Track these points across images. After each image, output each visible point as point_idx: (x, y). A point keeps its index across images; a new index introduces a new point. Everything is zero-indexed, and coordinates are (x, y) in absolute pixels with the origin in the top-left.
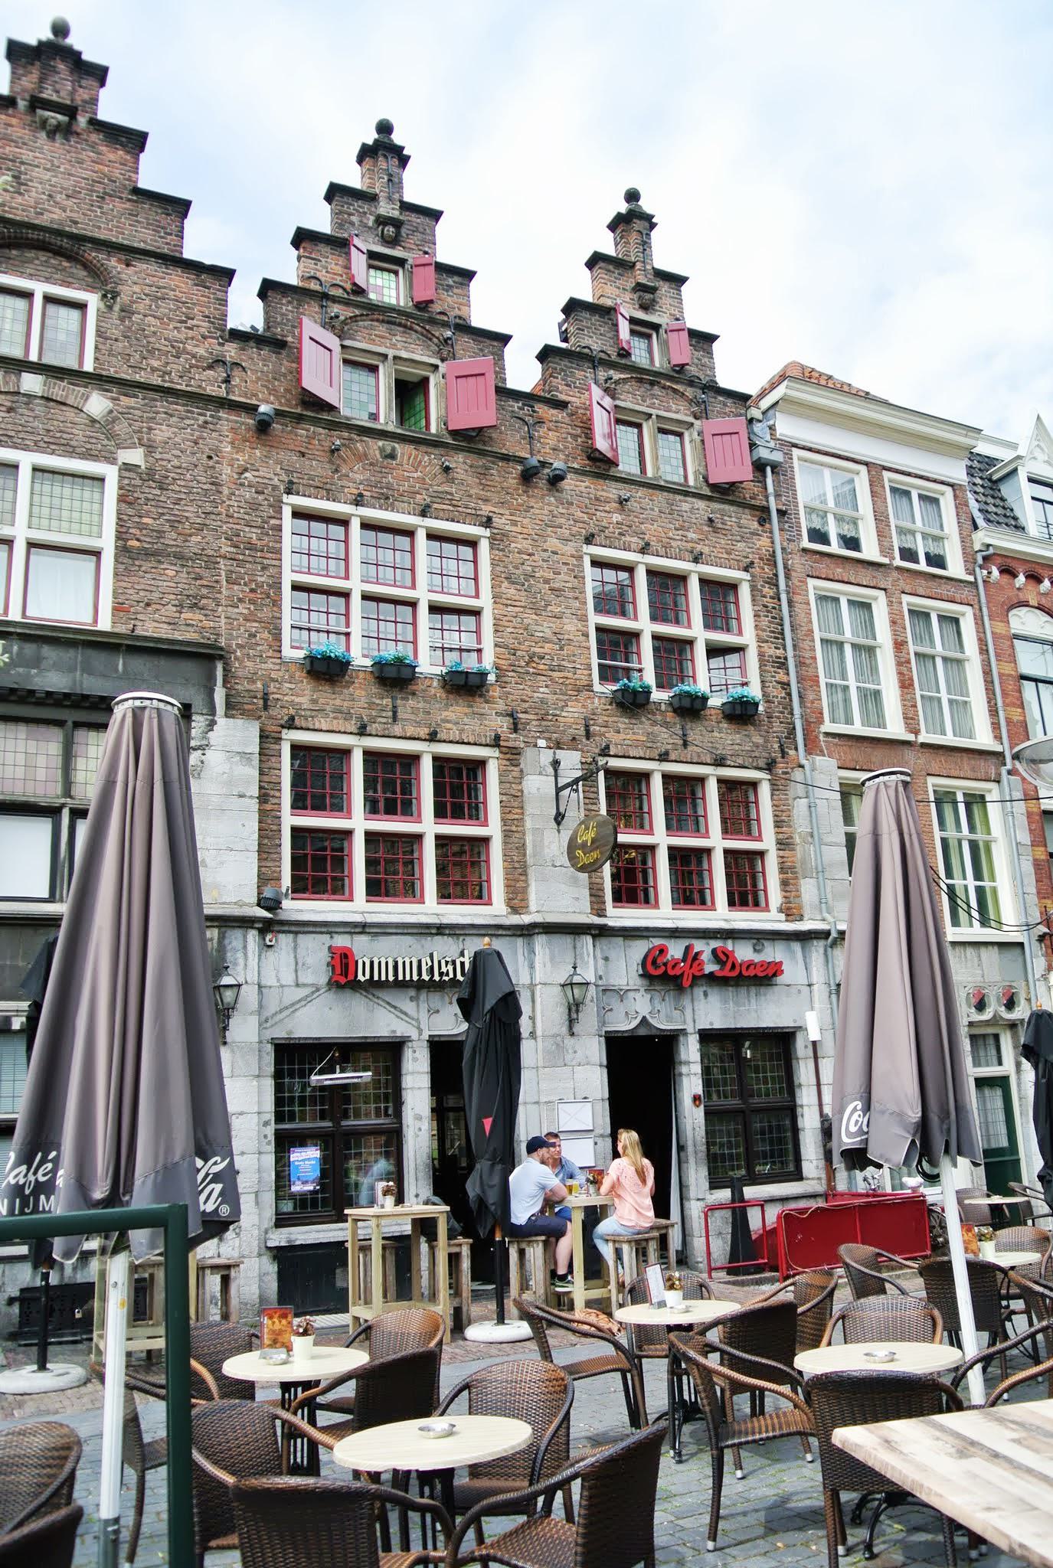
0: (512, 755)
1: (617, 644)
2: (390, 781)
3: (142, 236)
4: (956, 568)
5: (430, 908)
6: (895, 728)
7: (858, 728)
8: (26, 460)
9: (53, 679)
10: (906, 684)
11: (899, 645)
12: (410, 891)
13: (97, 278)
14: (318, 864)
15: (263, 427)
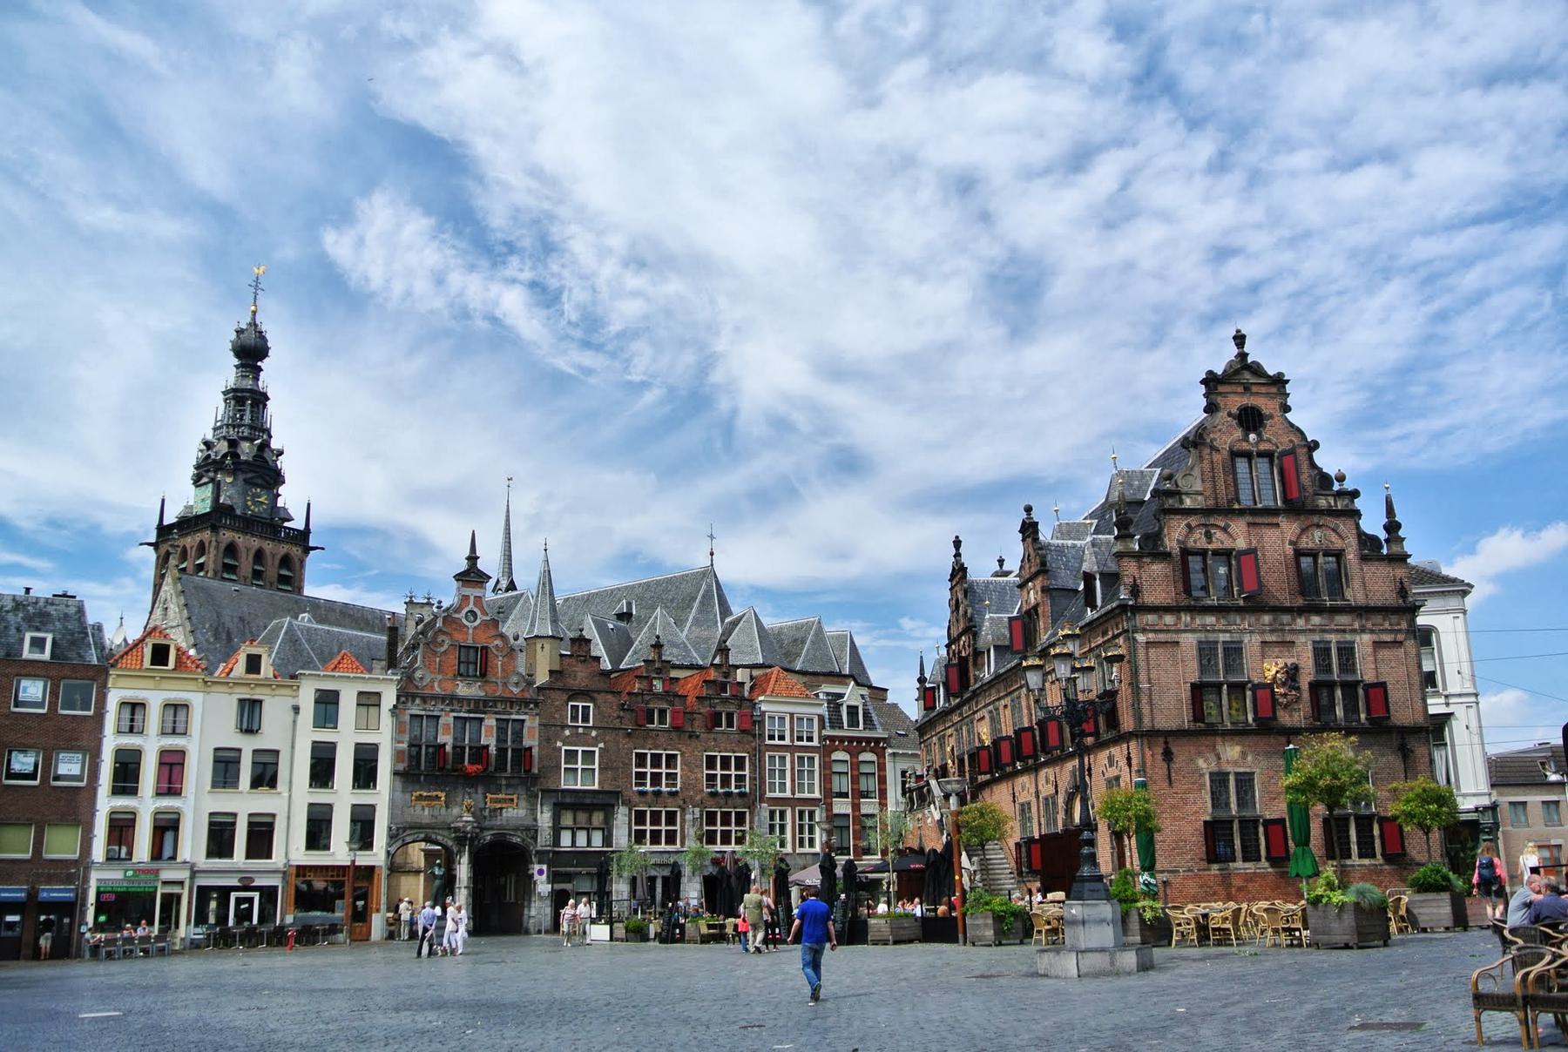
0: (683, 810)
1: (711, 778)
2: (656, 818)
3: (602, 685)
4: (815, 743)
5: (663, 847)
6: (788, 794)
7: (777, 794)
8: (580, 749)
9: (588, 801)
10: (793, 780)
11: (793, 769)
12: (659, 843)
13: (593, 700)
14: (640, 837)
15: (629, 735)
